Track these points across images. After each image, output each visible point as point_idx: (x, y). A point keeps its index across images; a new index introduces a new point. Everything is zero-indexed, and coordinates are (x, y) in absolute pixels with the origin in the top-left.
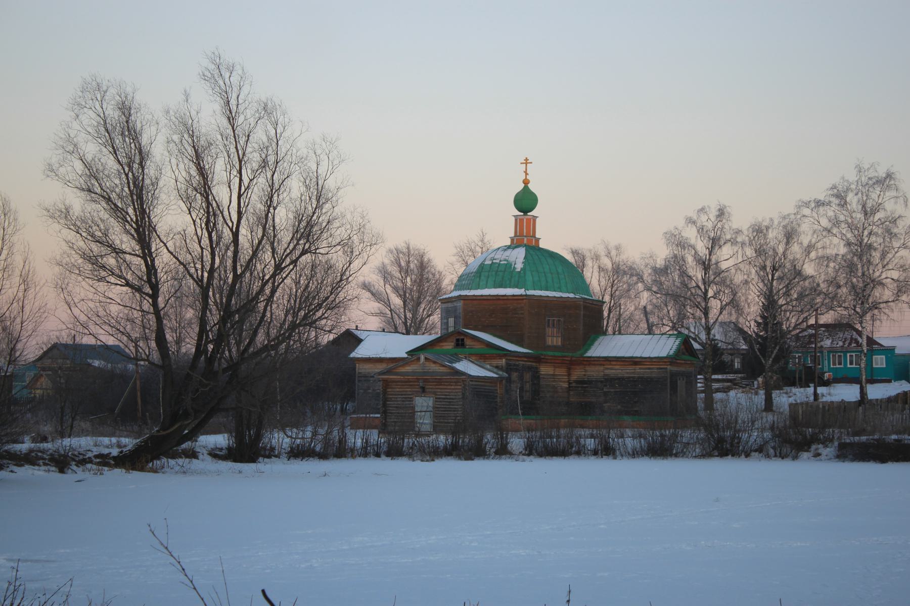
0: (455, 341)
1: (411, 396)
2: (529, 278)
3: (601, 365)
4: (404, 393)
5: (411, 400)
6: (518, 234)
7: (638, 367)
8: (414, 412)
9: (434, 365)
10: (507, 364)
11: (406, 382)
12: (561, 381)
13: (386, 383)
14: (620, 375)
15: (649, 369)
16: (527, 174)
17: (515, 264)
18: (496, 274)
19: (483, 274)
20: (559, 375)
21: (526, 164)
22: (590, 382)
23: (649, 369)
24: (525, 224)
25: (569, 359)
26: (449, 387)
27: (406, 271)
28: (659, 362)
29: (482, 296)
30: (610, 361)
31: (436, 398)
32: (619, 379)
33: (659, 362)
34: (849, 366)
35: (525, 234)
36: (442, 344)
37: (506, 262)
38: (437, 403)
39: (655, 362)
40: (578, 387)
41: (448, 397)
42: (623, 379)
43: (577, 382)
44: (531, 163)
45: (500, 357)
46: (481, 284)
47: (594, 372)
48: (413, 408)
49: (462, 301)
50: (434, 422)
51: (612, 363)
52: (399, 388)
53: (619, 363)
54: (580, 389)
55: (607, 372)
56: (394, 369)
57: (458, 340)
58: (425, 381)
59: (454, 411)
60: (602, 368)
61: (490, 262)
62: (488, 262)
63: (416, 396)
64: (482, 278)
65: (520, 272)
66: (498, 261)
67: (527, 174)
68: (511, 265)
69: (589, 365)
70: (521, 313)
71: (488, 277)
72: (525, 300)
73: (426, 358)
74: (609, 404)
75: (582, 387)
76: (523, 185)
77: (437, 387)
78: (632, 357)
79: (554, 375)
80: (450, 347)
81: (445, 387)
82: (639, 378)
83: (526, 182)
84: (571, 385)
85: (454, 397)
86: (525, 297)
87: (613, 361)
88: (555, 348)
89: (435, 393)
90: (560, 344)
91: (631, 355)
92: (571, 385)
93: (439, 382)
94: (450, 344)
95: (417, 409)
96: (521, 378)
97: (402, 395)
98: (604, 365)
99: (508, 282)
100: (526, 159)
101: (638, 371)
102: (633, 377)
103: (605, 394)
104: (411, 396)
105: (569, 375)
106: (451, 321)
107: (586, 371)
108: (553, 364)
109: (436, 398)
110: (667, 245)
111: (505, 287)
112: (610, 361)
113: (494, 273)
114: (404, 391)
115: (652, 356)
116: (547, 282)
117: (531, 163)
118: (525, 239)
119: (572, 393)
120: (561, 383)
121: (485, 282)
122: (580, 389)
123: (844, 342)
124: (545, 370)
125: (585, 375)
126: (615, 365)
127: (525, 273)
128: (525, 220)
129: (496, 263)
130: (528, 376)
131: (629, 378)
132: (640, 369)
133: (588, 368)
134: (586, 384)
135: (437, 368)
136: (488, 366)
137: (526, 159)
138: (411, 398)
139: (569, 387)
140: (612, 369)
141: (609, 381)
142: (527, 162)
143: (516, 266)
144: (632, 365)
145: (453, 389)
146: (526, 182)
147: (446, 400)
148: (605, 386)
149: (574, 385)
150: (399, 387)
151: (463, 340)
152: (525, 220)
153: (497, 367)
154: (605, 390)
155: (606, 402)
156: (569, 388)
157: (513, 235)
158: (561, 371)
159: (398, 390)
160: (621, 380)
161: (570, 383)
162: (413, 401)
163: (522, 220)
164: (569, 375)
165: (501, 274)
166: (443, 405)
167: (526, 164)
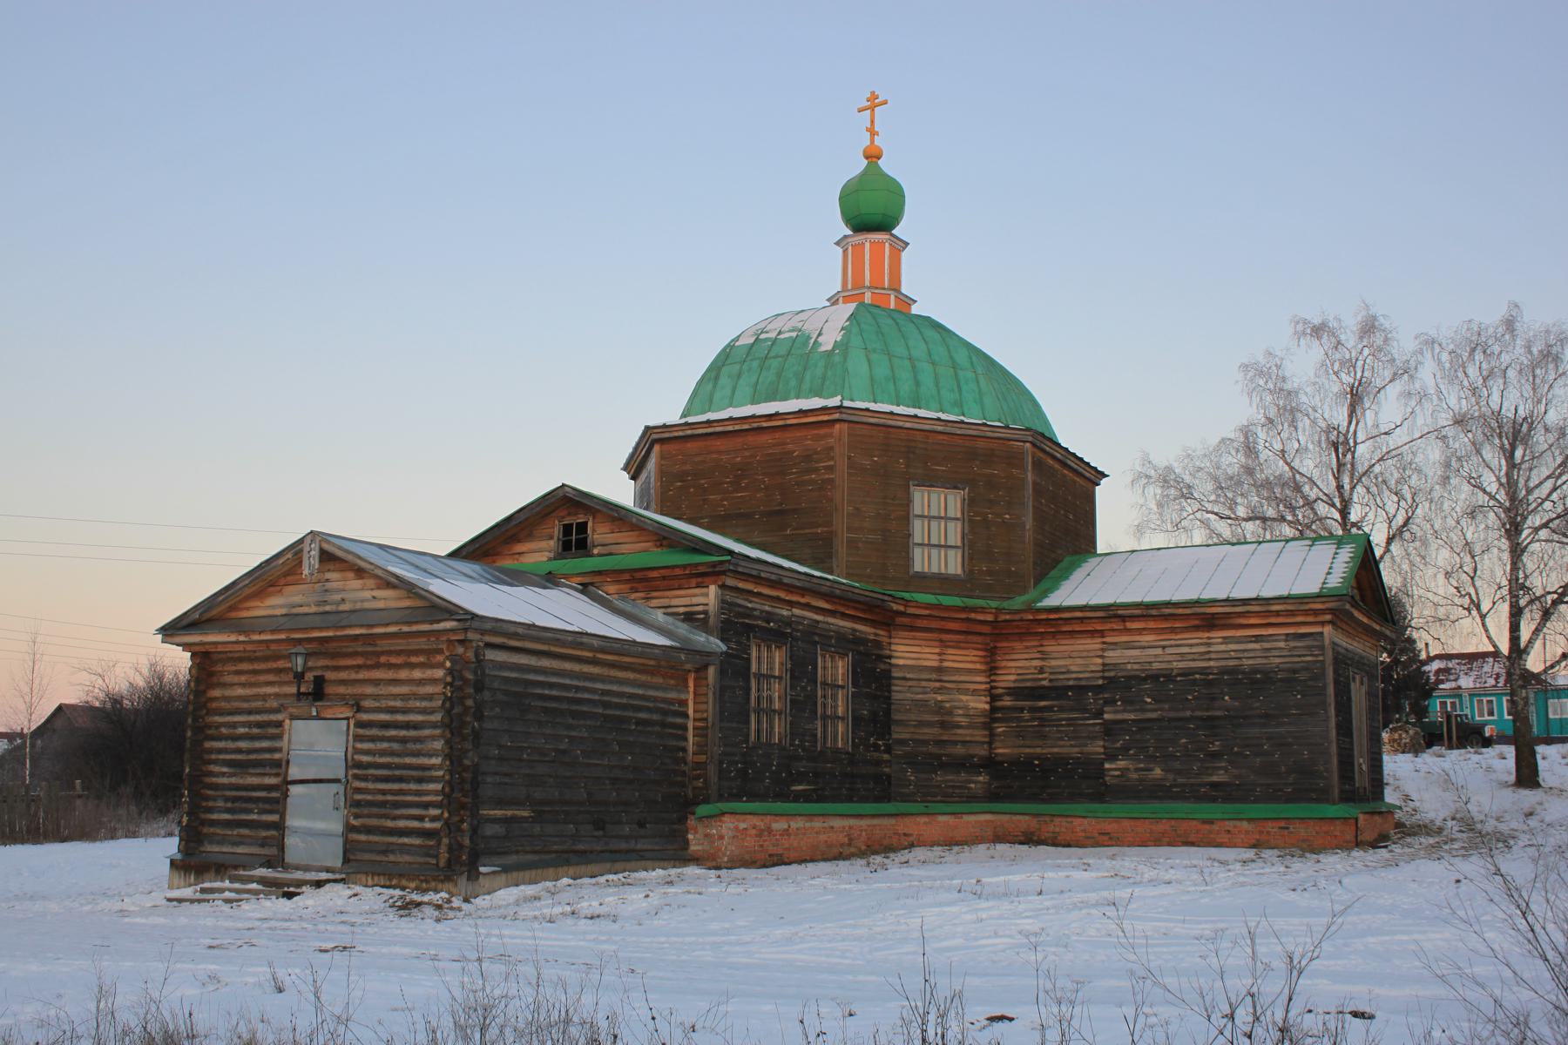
0: (557, 531)
1: (279, 717)
2: (858, 364)
4: (259, 704)
5: (274, 730)
6: (850, 287)
7: (1218, 634)
9: (357, 584)
10: (724, 605)
11: (266, 659)
12: (966, 692)
14: (1156, 666)
15: (1257, 639)
16: (873, 133)
17: (820, 334)
20: (958, 670)
22: (1057, 691)
23: (1257, 639)
24: (867, 257)
25: (990, 618)
26: (403, 674)
28: (1292, 613)
30: (1123, 618)
31: (360, 725)
32: (1154, 677)
33: (1292, 613)
34: (1477, 718)
35: (867, 283)
36: (519, 548)
37: (794, 334)
38: (359, 746)
39: (1277, 613)
40: (1022, 709)
41: (400, 717)
42: (1168, 676)
43: (1015, 692)
44: (885, 102)
45: (701, 576)
46: (717, 396)
48: (280, 766)
50: (349, 828)
51: (1130, 625)
52: (243, 685)
53: (1151, 625)
54: (1026, 715)
55: (1114, 656)
57: (567, 529)
58: (322, 648)
59: (420, 780)
60: (1093, 644)
63: (293, 718)
65: (830, 353)
67: (873, 133)
68: (809, 338)
69: (1054, 635)
70: (826, 468)
71: (739, 376)
72: (837, 426)
74: (1121, 764)
75: (1032, 709)
76: (866, 162)
77: (362, 675)
78: (1197, 603)
79: (939, 670)
80: (542, 557)
81: (390, 675)
82: (1224, 671)
83: (873, 155)
84: (999, 704)
85: (420, 718)
86: (837, 416)
87: (1133, 618)
88: (942, 582)
91: (1194, 596)
92: (999, 704)
94: (544, 544)
95: (294, 772)
96: (801, 671)
97: (250, 712)
98: (1102, 633)
99: (793, 383)
100: (874, 96)
101: (1220, 648)
102: (1202, 671)
103: (1109, 730)
104: (279, 717)
105: (992, 670)
107: (1044, 656)
108: (935, 635)
110: (1250, 395)
111: (785, 399)
112: (1123, 618)
113: (755, 364)
114: (256, 697)
115: (1267, 593)
116: (917, 383)
117: (885, 102)
119: (1000, 729)
120: (964, 698)
121: (728, 391)
122: (1026, 715)
123: (1496, 679)
124: (908, 653)
125: (1041, 670)
126: (1140, 631)
127: (845, 355)
128: (867, 245)
130: (838, 669)
131: (1186, 673)
132: (1226, 640)
133: (1051, 647)
134: (1042, 698)
135: (367, 594)
136: (659, 616)
137: (874, 96)
138: (279, 724)
139: (993, 709)
140: (1128, 646)
141: (1118, 685)
142: (873, 103)
143: (820, 339)
144: (1197, 628)
145: (421, 682)
146: (873, 155)
147: (393, 733)
148: (1107, 702)
149: (1007, 702)
150: (243, 679)
151: (582, 527)
152: (867, 245)
153: (689, 617)
154: (1106, 716)
155: (1112, 757)
156: (994, 714)
158: (965, 659)
159: (240, 691)
160: (1159, 680)
161: (994, 698)
162: (279, 737)
164: (992, 670)
165: (775, 363)
166: (383, 753)
167: (872, 108)
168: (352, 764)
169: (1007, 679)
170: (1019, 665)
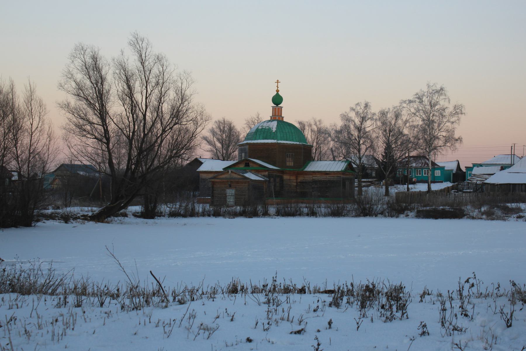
0: (245, 163)
2: (279, 135)
3: (311, 175)
5: (225, 190)
7: (328, 176)
8: (226, 196)
9: (235, 175)
10: (268, 174)
13: (213, 183)
15: (333, 176)
16: (278, 87)
18: (264, 133)
19: (257, 133)
21: (278, 82)
23: (333, 176)
26: (242, 185)
27: (223, 131)
29: (257, 143)
30: (315, 173)
31: (236, 190)
32: (319, 181)
34: (424, 175)
36: (239, 165)
42: (321, 181)
43: (300, 182)
45: (265, 171)
46: (257, 138)
47: (309, 178)
48: (226, 194)
49: (248, 146)
50: (235, 200)
54: (301, 186)
55: (314, 178)
56: (217, 176)
57: (246, 163)
58: (231, 182)
60: (311, 176)
61: (261, 128)
62: (260, 128)
64: (257, 135)
65: (274, 132)
66: (264, 127)
67: (278, 87)
71: (260, 135)
73: (231, 172)
79: (290, 179)
80: (243, 167)
82: (328, 180)
83: (278, 91)
88: (290, 167)
89: (236, 188)
90: (292, 165)
91: (325, 170)
93: (238, 182)
95: (227, 195)
96: (275, 181)
98: (312, 175)
101: (328, 177)
102: (326, 180)
105: (297, 179)
106: (243, 154)
107: (304, 178)
109: (236, 190)
110: (342, 120)
111: (268, 139)
112: (315, 173)
113: (263, 133)
115: (334, 170)
118: (277, 117)
123: (422, 164)
124: (286, 177)
125: (304, 179)
127: (277, 133)
128: (277, 109)
129: (264, 128)
130: (278, 180)
131: (324, 181)
132: (329, 176)
133: (305, 176)
136: (260, 175)
139: (297, 185)
141: (315, 182)
142: (278, 82)
146: (278, 91)
149: (299, 184)
151: (248, 163)
152: (277, 109)
153: (264, 176)
156: (297, 185)
157: (271, 115)
158: (293, 178)
160: (320, 181)
163: (275, 109)
164: (297, 179)
167: (278, 82)
168: (235, 194)
169: (299, 180)
170: (300, 179)
